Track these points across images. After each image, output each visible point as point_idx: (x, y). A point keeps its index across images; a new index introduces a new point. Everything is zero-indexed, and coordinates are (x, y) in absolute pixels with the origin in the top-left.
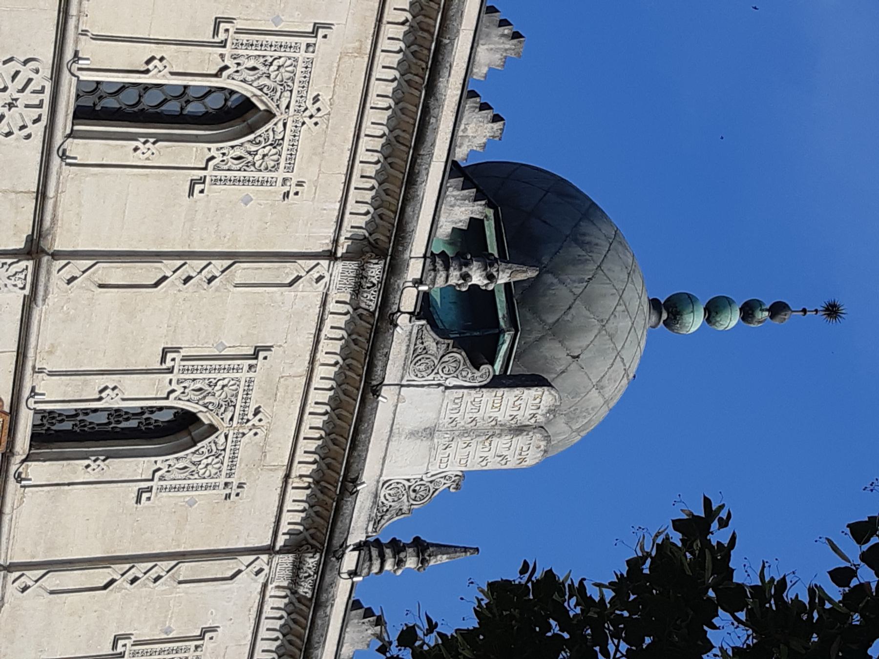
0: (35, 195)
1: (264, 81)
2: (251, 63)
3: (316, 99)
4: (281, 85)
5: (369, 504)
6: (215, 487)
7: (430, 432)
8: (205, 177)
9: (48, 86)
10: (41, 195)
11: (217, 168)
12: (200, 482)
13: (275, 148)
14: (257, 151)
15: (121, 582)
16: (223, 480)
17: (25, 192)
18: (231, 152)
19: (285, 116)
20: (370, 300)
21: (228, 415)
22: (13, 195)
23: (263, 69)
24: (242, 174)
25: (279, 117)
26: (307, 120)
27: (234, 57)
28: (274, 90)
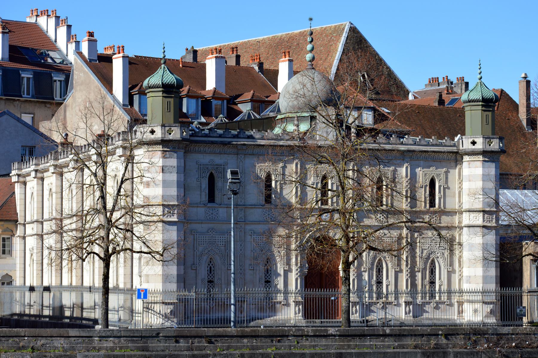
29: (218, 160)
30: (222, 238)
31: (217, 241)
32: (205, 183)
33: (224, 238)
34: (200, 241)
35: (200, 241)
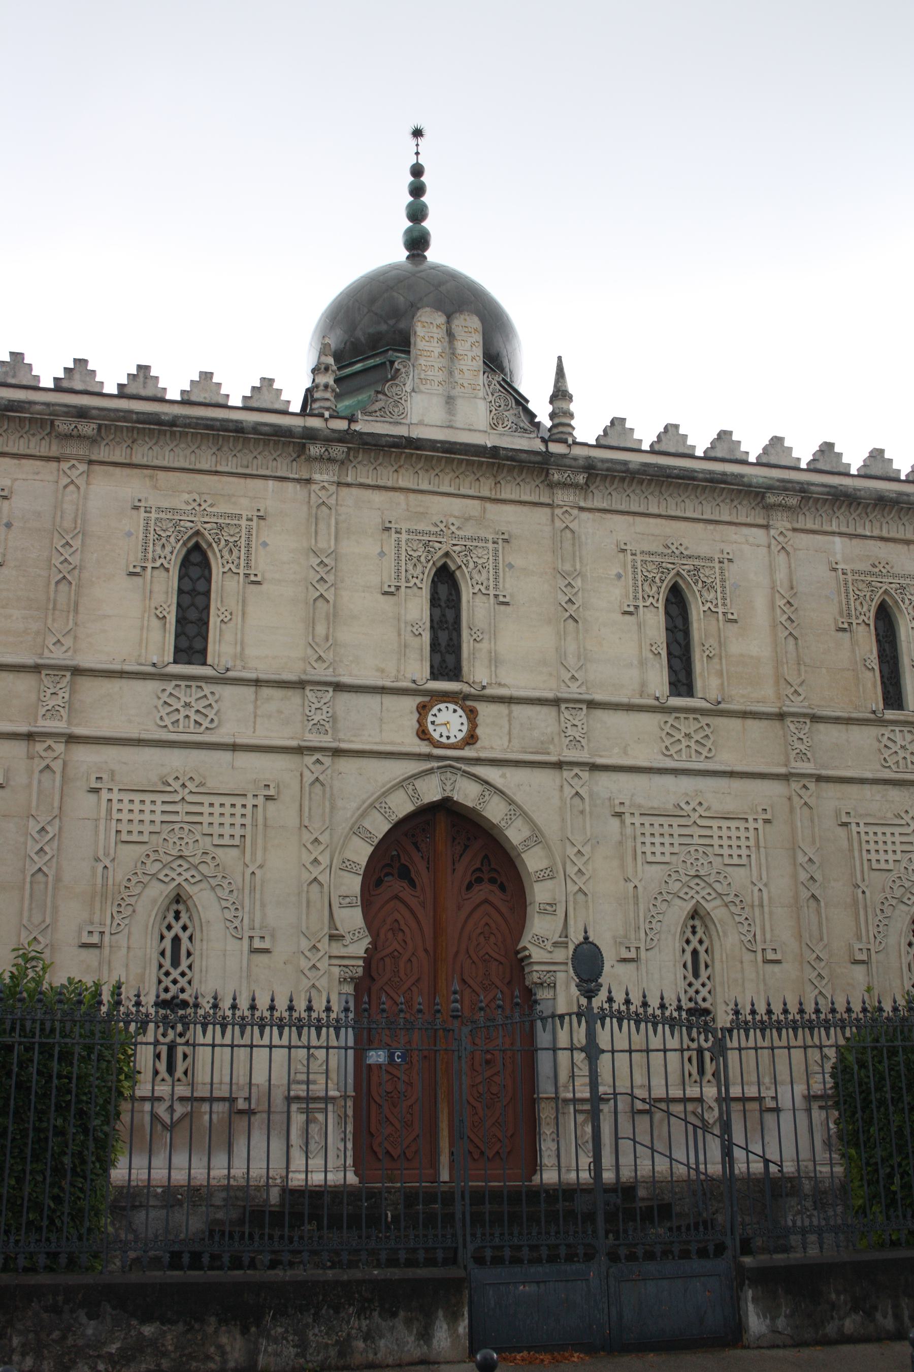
1: (172, 540)
2: (158, 549)
3: (187, 503)
5: (509, 439)
6: (496, 550)
7: (450, 400)
9: (174, 683)
10: (257, 683)
11: (238, 566)
12: (491, 561)
15: (572, 610)
16: (490, 546)
19: (199, 524)
20: (338, 451)
21: (437, 545)
22: (259, 703)
23: (164, 540)
24: (243, 550)
25: (199, 527)
27: (154, 560)
28: (179, 532)
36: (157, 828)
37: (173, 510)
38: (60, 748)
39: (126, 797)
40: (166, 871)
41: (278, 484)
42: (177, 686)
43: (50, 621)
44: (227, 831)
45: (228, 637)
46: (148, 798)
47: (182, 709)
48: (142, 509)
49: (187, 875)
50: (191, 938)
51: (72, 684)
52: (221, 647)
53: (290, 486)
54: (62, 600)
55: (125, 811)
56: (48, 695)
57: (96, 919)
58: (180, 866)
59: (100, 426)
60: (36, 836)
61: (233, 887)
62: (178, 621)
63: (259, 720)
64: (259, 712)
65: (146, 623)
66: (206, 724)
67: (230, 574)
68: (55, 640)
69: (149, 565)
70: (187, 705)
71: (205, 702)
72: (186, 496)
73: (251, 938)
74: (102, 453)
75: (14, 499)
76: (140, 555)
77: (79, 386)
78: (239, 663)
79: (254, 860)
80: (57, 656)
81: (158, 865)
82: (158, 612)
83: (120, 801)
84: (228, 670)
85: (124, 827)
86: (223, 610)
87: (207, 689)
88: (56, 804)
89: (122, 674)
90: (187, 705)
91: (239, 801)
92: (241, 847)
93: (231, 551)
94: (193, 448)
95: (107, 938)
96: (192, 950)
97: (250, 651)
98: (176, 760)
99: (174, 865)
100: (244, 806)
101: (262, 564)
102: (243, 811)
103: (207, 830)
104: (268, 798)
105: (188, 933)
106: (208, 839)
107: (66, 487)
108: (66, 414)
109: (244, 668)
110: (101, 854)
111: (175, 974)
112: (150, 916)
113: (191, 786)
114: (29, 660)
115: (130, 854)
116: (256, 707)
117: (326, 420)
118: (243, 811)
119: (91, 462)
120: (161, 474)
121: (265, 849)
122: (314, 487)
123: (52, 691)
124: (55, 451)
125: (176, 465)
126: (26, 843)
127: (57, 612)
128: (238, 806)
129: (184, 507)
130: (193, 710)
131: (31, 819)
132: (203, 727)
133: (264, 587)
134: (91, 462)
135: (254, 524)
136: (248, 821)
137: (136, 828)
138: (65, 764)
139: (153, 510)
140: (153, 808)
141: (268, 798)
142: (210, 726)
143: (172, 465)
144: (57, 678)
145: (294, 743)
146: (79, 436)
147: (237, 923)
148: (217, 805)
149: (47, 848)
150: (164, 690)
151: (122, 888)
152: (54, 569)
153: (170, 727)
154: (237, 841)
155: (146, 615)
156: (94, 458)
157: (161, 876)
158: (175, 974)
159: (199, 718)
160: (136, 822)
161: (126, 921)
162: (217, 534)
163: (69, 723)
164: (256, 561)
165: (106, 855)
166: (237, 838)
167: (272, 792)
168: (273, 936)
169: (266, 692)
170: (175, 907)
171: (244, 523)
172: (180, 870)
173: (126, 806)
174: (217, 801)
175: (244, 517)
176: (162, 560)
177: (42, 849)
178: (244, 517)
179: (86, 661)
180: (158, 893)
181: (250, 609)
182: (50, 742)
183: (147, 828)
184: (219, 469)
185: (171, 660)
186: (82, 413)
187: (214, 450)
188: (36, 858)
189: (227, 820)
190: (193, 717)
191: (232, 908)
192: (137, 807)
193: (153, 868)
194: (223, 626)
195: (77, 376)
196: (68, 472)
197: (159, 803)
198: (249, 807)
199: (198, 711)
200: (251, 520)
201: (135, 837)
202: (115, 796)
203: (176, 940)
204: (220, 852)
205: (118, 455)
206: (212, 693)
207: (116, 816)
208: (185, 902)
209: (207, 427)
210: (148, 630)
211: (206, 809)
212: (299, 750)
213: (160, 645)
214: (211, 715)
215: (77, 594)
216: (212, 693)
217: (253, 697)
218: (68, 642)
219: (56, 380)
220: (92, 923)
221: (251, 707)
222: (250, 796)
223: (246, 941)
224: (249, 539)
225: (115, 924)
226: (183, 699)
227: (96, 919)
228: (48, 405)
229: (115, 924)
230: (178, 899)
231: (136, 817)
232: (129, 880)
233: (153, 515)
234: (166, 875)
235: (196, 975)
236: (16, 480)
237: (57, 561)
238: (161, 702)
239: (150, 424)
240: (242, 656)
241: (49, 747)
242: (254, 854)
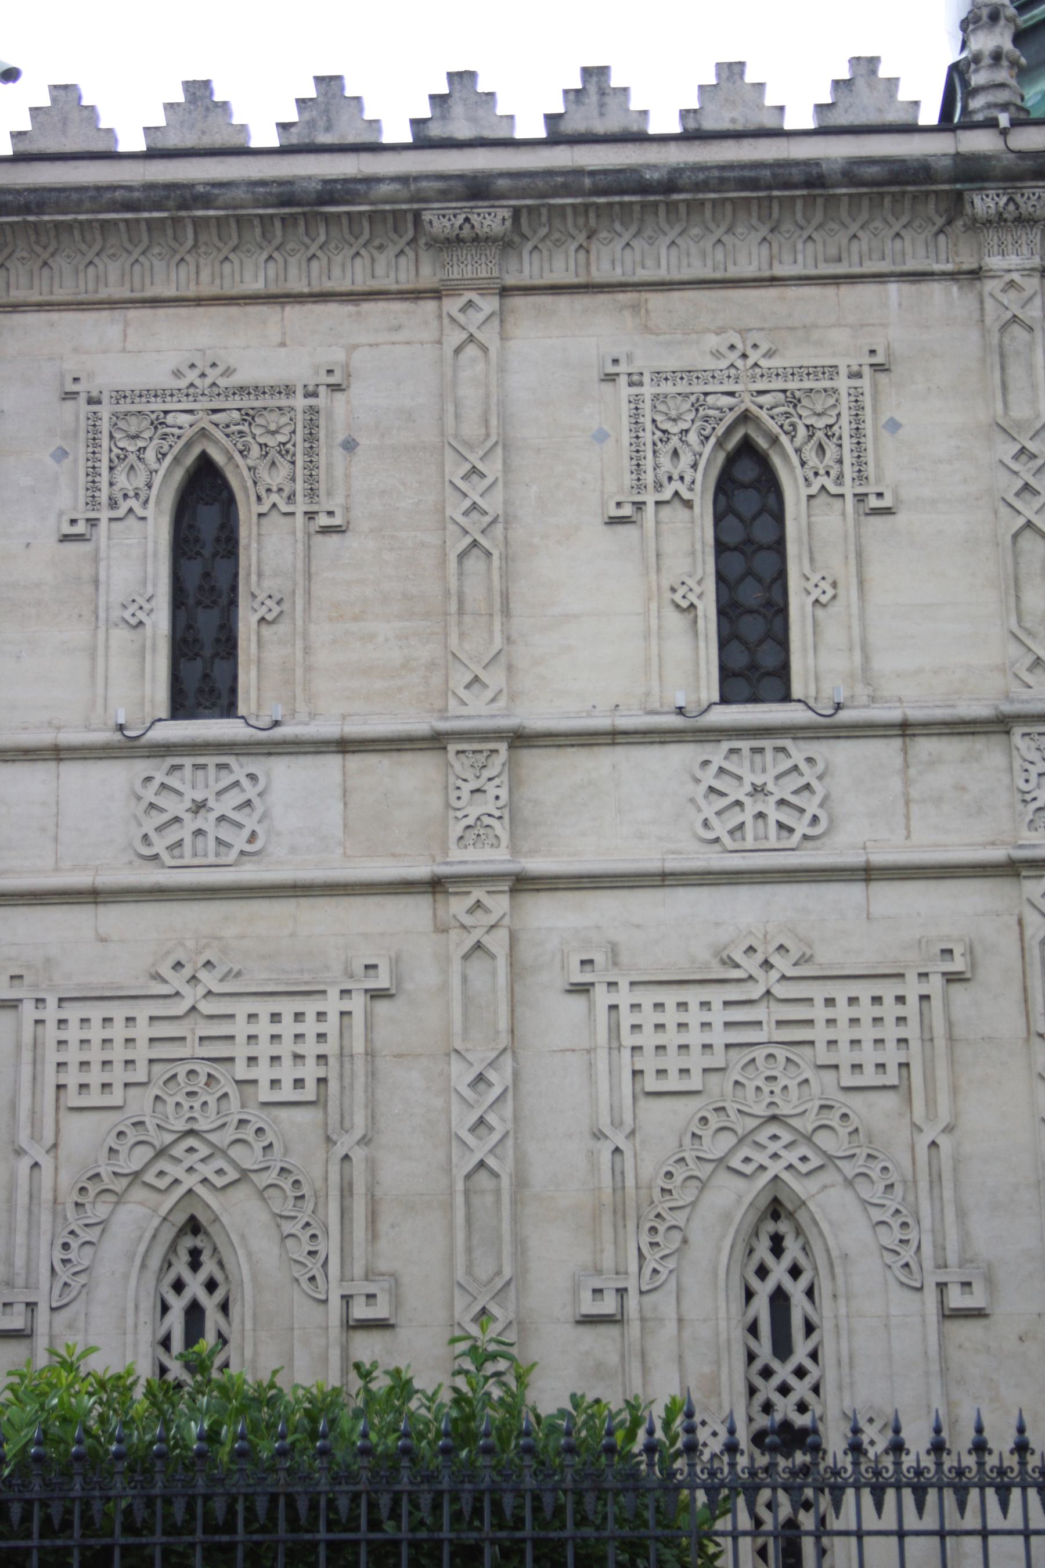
0: (907, 739)
1: (693, 438)
2: (665, 460)
3: (717, 354)
4: (697, 410)
8: (855, 495)
9: (726, 745)
10: (905, 729)
11: (839, 479)
13: (799, 401)
14: (807, 426)
17: (906, 753)
18: (811, 464)
19: (747, 397)
22: (912, 772)
23: (675, 441)
25: (748, 404)
26: (750, 362)
27: (659, 486)
28: (706, 419)
29: (265, 349)
30: (288, 1028)
31: (240, 1051)
32: (139, 557)
33: (310, 1027)
34: (73, 1055)
35: (73, 1055)
36: (717, 1059)
37: (689, 374)
38: (500, 904)
39: (647, 998)
40: (746, 1151)
41: (907, 288)
42: (732, 751)
43: (454, 639)
44: (868, 1055)
45: (834, 634)
46: (693, 996)
47: (747, 801)
48: (623, 380)
49: (791, 1157)
50: (810, 1293)
51: (512, 765)
52: (819, 658)
53: (936, 289)
54: (475, 592)
55: (648, 1028)
56: (465, 794)
57: (608, 1261)
58: (775, 1137)
59: (517, 212)
60: (468, 1093)
61: (893, 1177)
62: (721, 612)
63: (914, 808)
64: (914, 793)
65: (654, 623)
66: (802, 827)
67: (823, 498)
68: (469, 677)
69: (650, 498)
70: (758, 790)
71: (795, 782)
72: (712, 341)
73: (942, 1286)
74: (528, 269)
75: (356, 388)
76: (628, 479)
77: (462, 130)
78: (862, 692)
79: (931, 1114)
80: (477, 711)
81: (727, 1141)
82: (678, 597)
83: (635, 1007)
84: (838, 707)
85: (648, 1063)
86: (815, 578)
87: (798, 751)
88: (503, 1024)
89: (614, 737)
90: (758, 790)
91: (888, 990)
92: (902, 1089)
93: (821, 448)
94: (719, 233)
95: (632, 1301)
96: (814, 1318)
97: (883, 663)
98: (745, 911)
99: (762, 1137)
100: (901, 999)
101: (892, 469)
102: (900, 1011)
103: (824, 1057)
104: (952, 978)
105: (803, 1282)
106: (829, 1076)
107: (458, 351)
108: (444, 195)
109: (873, 699)
110: (604, 1123)
111: (783, 1372)
112: (719, 1250)
113: (782, 964)
114: (420, 725)
115: (665, 1120)
116: (907, 782)
117: (1004, 132)
118: (900, 1011)
119: (505, 292)
120: (655, 300)
121: (955, 1090)
122: (991, 286)
123: (474, 785)
124: (428, 275)
125: (686, 274)
126: (448, 1112)
127: (467, 619)
128: (889, 1000)
129: (711, 363)
130: (772, 800)
131: (453, 1056)
132: (797, 837)
133: (901, 519)
134: (505, 292)
135: (865, 383)
136: (912, 1031)
137: (672, 1062)
138: (513, 939)
139: (646, 379)
140: (706, 1017)
141: (952, 978)
142: (810, 832)
143: (676, 276)
144: (481, 758)
145: (998, 854)
146: (476, 239)
147: (907, 1254)
148: (842, 1001)
149: (492, 1119)
150: (706, 763)
151: (656, 1194)
152: (451, 527)
153: (726, 839)
154: (892, 1077)
155: (654, 606)
156: (510, 280)
157: (736, 1162)
158: (783, 1372)
159: (787, 817)
160: (672, 1050)
161: (671, 1263)
162: (788, 415)
163: (514, 849)
164: (877, 465)
165: (617, 1124)
166: (892, 1069)
167: (958, 964)
168: (989, 1280)
169: (925, 747)
170: (770, 1227)
171: (843, 383)
172: (774, 1147)
173: (648, 1017)
174: (841, 992)
175: (843, 371)
176: (676, 485)
177: (481, 1121)
178: (843, 371)
179: (537, 716)
180: (732, 1199)
181: (874, 571)
182: (478, 893)
183: (696, 1061)
184: (779, 271)
185: (716, 697)
186: (477, 189)
187: (764, 231)
188: (470, 1139)
189: (867, 1033)
190: (775, 815)
191: (895, 1223)
192: (671, 1017)
193: (719, 1146)
194: (820, 612)
195: (458, 109)
196: (461, 318)
197: (717, 1005)
198: (912, 1000)
199: (782, 802)
200: (858, 375)
201: (673, 1083)
202: (624, 997)
203: (780, 1299)
204: (856, 1101)
205: (561, 268)
206: (810, 760)
207: (628, 1040)
208: (791, 1215)
209: (744, 184)
210: (660, 637)
211: (819, 1013)
212: (1012, 869)
213: (688, 666)
214: (812, 809)
215: (506, 575)
216: (810, 760)
217: (899, 761)
218: (495, 679)
219: (417, 124)
220: (599, 1272)
221: (896, 784)
222: (911, 977)
223: (931, 1295)
224: (857, 417)
225: (647, 1272)
226: (749, 778)
227: (608, 1261)
228: (404, 179)
229: (647, 1272)
230: (775, 1210)
231: (672, 1038)
232: (669, 1175)
233: (648, 390)
234: (747, 1160)
235: (829, 1372)
236: (355, 347)
237: (455, 509)
238: (703, 788)
239: (623, 192)
240: (866, 674)
241: (478, 904)
242: (930, 1102)
